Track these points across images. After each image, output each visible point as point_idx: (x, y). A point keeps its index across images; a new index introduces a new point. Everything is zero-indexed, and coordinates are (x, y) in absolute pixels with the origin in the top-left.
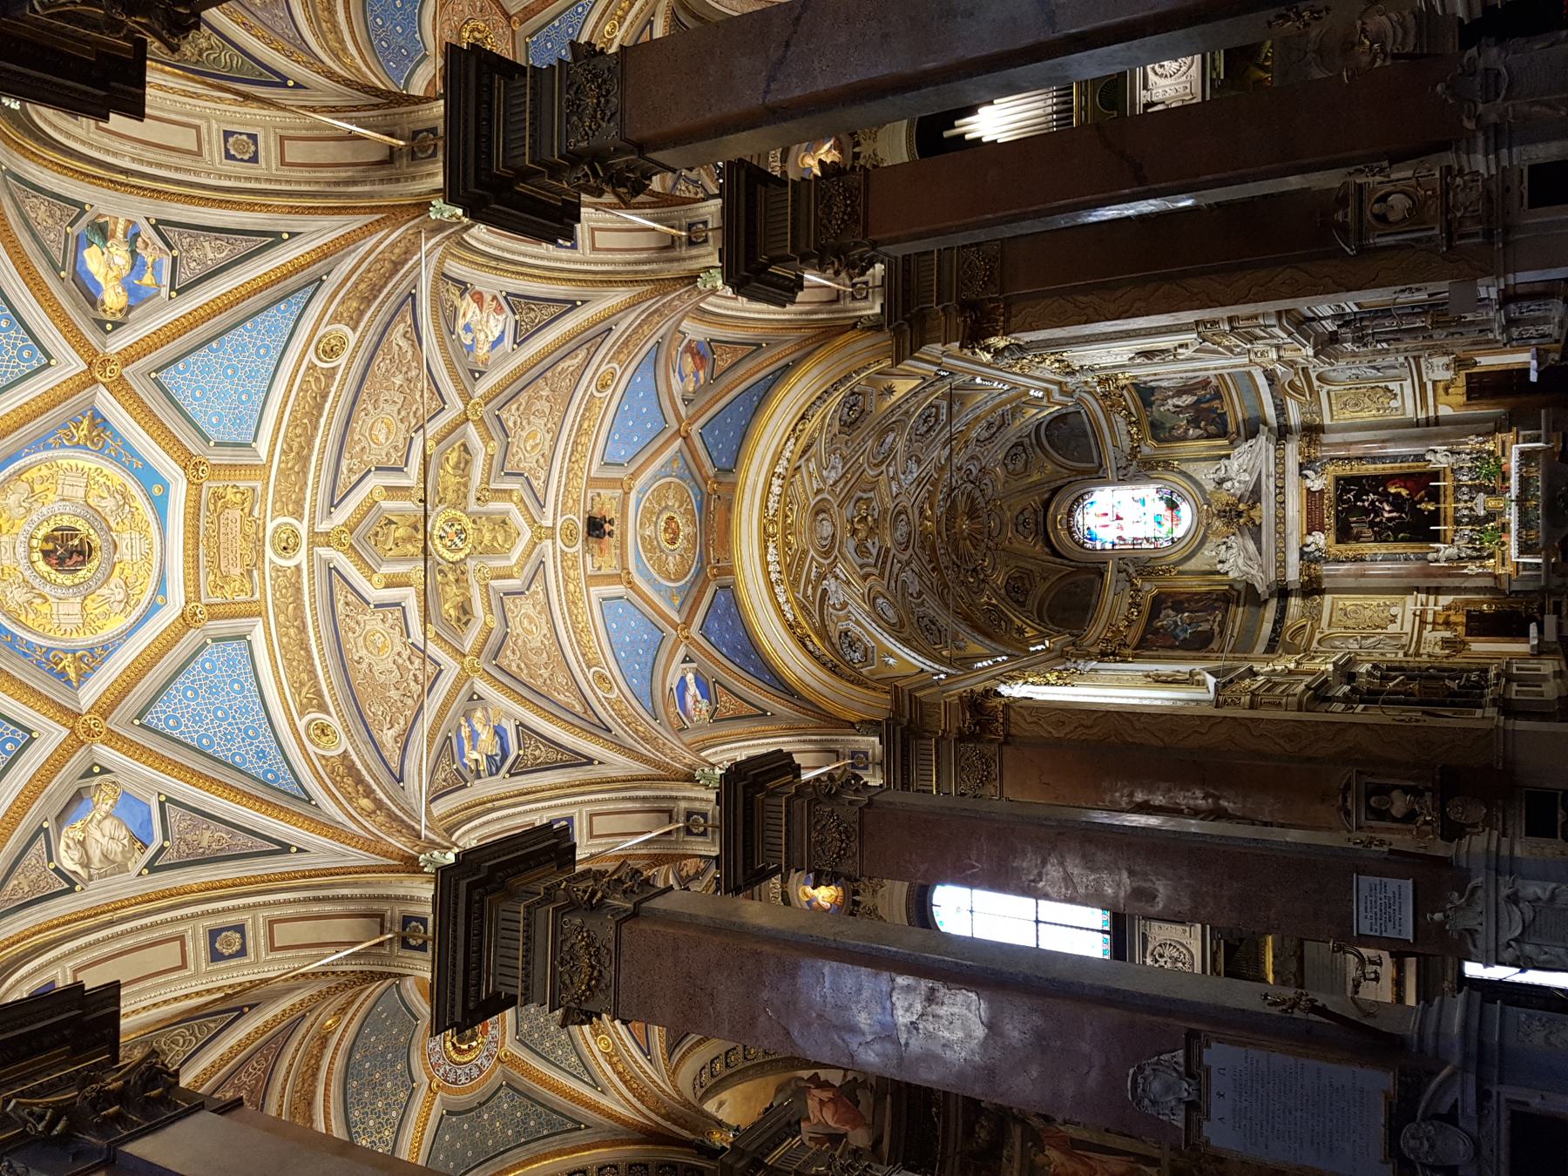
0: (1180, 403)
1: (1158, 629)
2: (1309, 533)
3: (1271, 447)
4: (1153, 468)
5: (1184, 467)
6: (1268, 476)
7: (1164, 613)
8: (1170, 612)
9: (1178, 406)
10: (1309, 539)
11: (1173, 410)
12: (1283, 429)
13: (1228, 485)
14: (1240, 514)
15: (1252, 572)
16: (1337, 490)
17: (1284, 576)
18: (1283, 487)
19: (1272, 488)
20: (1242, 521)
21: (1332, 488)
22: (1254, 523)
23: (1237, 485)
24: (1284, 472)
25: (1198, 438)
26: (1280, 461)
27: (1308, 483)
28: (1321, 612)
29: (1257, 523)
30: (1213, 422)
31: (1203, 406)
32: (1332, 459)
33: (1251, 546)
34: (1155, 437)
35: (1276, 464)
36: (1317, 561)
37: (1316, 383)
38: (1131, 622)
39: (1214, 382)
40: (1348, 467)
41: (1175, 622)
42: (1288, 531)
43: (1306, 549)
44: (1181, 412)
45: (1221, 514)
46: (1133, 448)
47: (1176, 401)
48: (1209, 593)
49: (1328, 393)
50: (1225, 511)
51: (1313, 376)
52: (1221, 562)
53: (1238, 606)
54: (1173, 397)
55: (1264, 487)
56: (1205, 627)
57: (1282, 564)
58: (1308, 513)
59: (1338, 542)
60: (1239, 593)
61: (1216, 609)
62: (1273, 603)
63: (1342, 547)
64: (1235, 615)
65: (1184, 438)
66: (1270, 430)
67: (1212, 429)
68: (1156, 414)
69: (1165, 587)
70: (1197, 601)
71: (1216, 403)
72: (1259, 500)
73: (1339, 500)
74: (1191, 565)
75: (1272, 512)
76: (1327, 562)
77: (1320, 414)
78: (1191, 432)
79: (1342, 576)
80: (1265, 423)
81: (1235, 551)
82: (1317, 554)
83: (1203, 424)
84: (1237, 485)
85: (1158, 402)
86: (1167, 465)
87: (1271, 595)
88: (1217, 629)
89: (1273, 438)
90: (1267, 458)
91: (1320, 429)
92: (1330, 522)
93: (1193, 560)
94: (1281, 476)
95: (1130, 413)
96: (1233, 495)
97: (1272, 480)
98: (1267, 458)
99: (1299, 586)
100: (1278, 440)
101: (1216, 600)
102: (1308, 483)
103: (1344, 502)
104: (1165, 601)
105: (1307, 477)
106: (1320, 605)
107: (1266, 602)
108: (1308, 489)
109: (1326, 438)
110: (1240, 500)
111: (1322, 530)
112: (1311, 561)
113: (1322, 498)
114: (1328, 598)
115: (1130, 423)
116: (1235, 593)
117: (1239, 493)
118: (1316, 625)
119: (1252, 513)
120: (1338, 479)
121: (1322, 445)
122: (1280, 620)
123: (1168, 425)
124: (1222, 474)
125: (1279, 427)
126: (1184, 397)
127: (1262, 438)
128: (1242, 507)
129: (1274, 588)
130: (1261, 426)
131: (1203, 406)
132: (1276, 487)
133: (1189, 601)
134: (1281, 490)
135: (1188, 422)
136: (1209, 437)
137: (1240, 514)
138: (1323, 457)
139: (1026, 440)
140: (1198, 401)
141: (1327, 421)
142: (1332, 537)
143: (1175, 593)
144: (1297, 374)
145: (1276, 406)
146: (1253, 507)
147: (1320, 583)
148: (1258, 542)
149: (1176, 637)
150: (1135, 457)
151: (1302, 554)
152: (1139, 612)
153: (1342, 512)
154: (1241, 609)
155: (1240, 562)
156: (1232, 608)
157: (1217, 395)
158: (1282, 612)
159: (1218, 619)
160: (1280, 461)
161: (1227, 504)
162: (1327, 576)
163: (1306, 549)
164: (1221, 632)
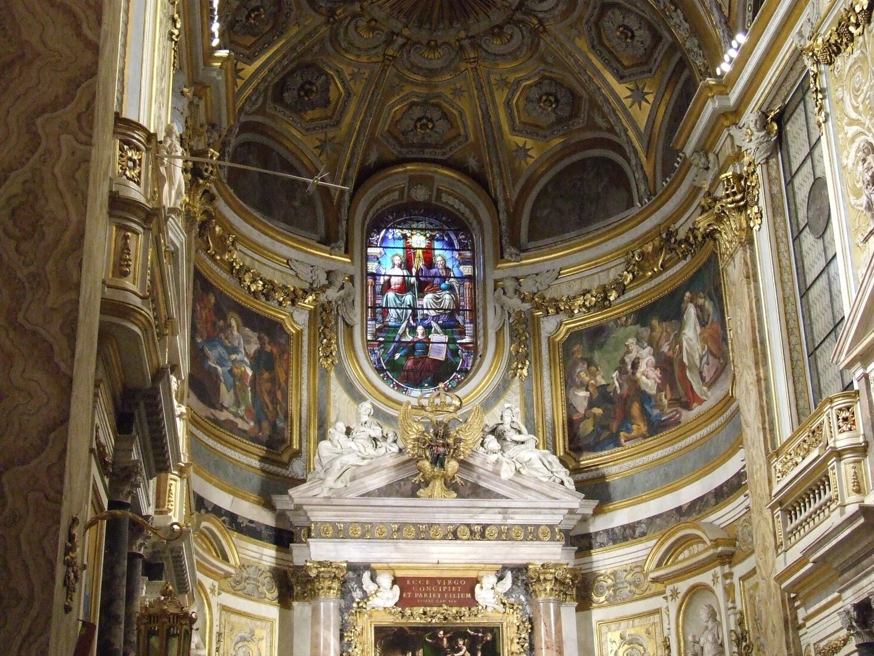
0: (643, 367)
1: (225, 318)
2: (395, 581)
3: (556, 519)
4: (515, 335)
5: (516, 385)
6: (505, 510)
7: (254, 336)
8: (254, 347)
9: (635, 365)
10: (385, 580)
11: (628, 360)
12: (584, 542)
13: (492, 442)
14: (438, 460)
15: (330, 481)
16: (476, 629)
17: (319, 536)
18: (483, 536)
19: (484, 519)
20: (427, 464)
21: (480, 620)
22: (418, 486)
23: (493, 458)
24: (511, 539)
25: (570, 407)
26: (531, 533)
27: (489, 580)
28: (248, 596)
29: (421, 492)
30: (601, 425)
31: (635, 409)
32: (530, 620)
33: (377, 481)
34: (574, 336)
35: (524, 527)
36: (345, 593)
37: (683, 586)
38: (237, 273)
39: (687, 416)
40: (516, 648)
41: (235, 350)
42: (402, 544)
43: (366, 576)
44: (622, 369)
45: (442, 431)
46: (555, 302)
47: (647, 357)
48: (287, 416)
49: (657, 611)
50: (446, 435)
51: (705, 578)
52: (348, 432)
53: (263, 459)
54: (657, 354)
55: (486, 503)
56: (227, 397)
57: (340, 533)
58: (433, 580)
59: (379, 630)
60: (286, 465)
61: (258, 422)
62: (266, 518)
63: (370, 636)
64: (247, 452)
65: (570, 382)
66: (584, 519)
67: (587, 427)
68: (620, 332)
69: (299, 345)
70: (272, 394)
71: (639, 427)
72: (460, 496)
73: (457, 633)
74: (337, 393)
75: (440, 518)
76: (341, 611)
77: (612, 602)
78: (583, 394)
79: (315, 636)
80: (598, 512)
81: (370, 451)
82: (357, 595)
83: (598, 411)
84: (493, 458)
85: (645, 332)
86: (519, 358)
87: (281, 516)
88: (223, 416)
89: (571, 524)
90: (537, 510)
91: (584, 603)
92: (416, 617)
93: (345, 397)
94: (505, 534)
95: (622, 290)
96: (474, 452)
97: (498, 519)
98: (537, 510)
99: (298, 560)
100: (566, 532)
101: (274, 426)
102: (489, 580)
103: (452, 640)
104: (273, 341)
105: (500, 579)
106: (261, 598)
107: (269, 505)
108: (477, 581)
109: (569, 612)
110: (465, 465)
111: (402, 602)
112: (344, 583)
113: (460, 603)
114: (273, 612)
115: (605, 291)
116: (285, 458)
117: (476, 461)
118: (226, 584)
119: (438, 484)
120: (495, 631)
121: (559, 603)
122: (233, 522)
123: (597, 355)
124: (511, 435)
125: (588, 536)
126: (655, 374)
127: (575, 501)
128: (452, 466)
129: (297, 520)
130: (594, 503)
131: (635, 409)
132: (485, 527)
133: (274, 380)
134: (480, 533)
135: (603, 386)
136: (571, 425)
137: (438, 460)
138: (535, 605)
139: (581, 121)
140: (644, 398)
141: (597, 615)
142: (387, 620)
143: (288, 362)
144: (716, 543)
145: (632, 527)
146: (451, 485)
147: (302, 597)
148: (384, 492)
149: (211, 340)
150: (538, 307)
151: (357, 569)
152: (255, 294)
153: (434, 636)
154: (256, 463)
155: (351, 459)
156: (261, 450)
157: (655, 427)
158: (252, 531)
159: (241, 424)
160: (531, 533)
161: (458, 441)
162: (315, 611)
163: (366, 576)
164: (216, 422)
